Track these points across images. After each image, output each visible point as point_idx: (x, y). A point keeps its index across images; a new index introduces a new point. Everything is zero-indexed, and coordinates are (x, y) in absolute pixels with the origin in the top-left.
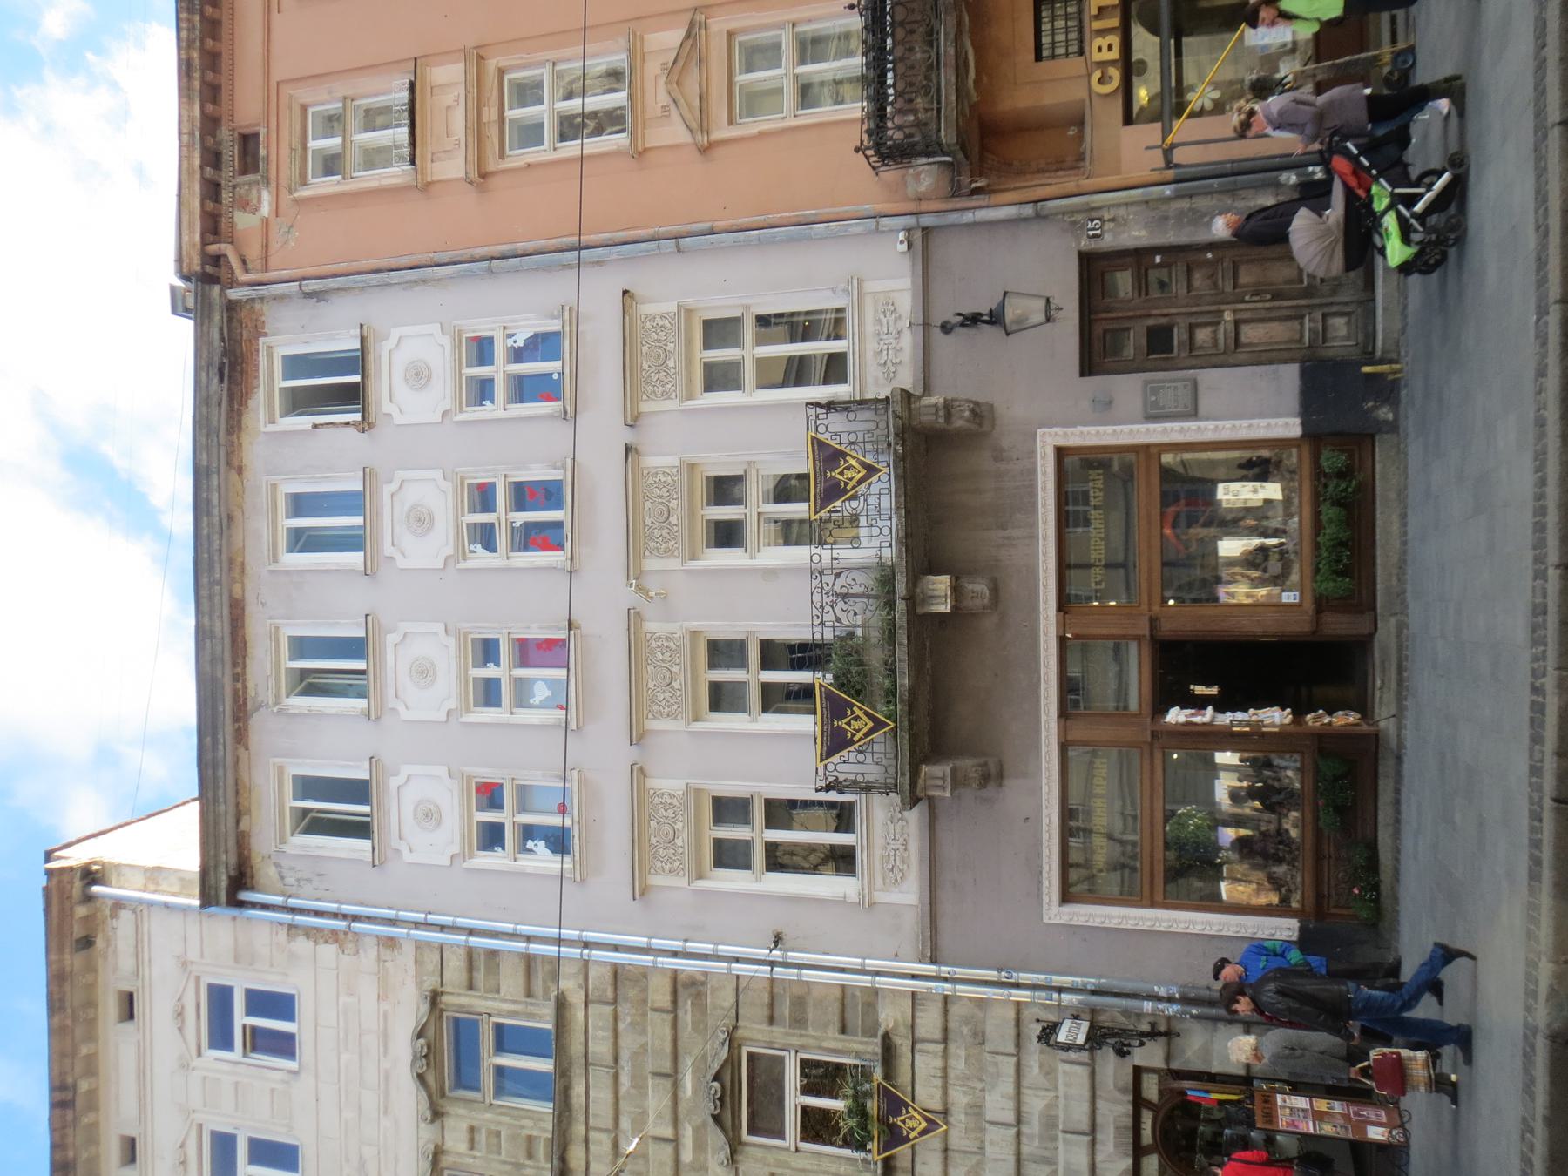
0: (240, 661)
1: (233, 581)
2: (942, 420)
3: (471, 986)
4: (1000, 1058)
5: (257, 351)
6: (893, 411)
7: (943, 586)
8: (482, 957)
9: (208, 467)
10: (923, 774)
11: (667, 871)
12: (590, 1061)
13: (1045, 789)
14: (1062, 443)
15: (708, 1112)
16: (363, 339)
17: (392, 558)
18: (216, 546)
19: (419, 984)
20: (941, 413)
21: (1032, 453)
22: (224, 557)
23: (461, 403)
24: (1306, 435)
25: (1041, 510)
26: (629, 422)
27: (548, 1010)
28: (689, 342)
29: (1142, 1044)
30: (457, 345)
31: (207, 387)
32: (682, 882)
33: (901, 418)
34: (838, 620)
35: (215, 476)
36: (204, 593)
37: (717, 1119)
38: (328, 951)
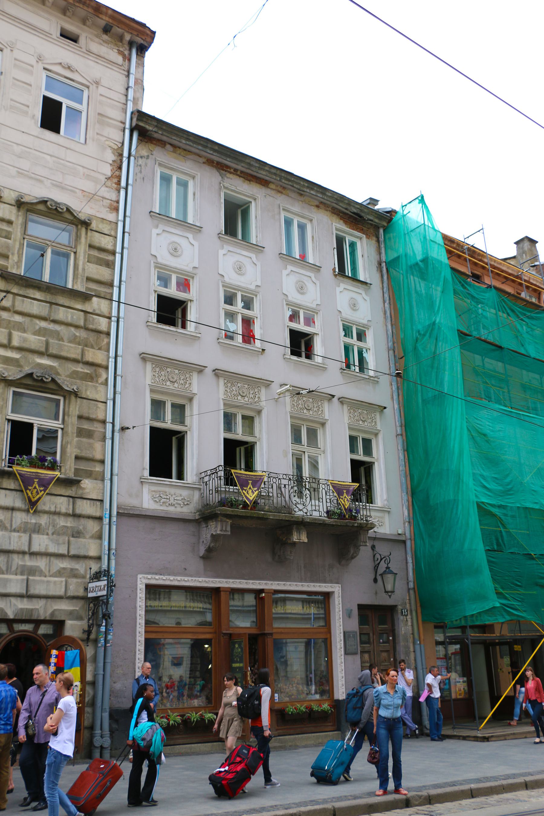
0: (242, 175)
1: (277, 186)
4: (67, 546)
10: (228, 520)
11: (154, 374)
12: (54, 306)
13: (200, 579)
15: (34, 371)
17: (286, 269)
18: (295, 185)
22: (290, 187)
23: (359, 326)
27: (80, 287)
31: (354, 206)
32: (148, 381)
36: (278, 172)
37: (30, 375)
38: (108, 170)
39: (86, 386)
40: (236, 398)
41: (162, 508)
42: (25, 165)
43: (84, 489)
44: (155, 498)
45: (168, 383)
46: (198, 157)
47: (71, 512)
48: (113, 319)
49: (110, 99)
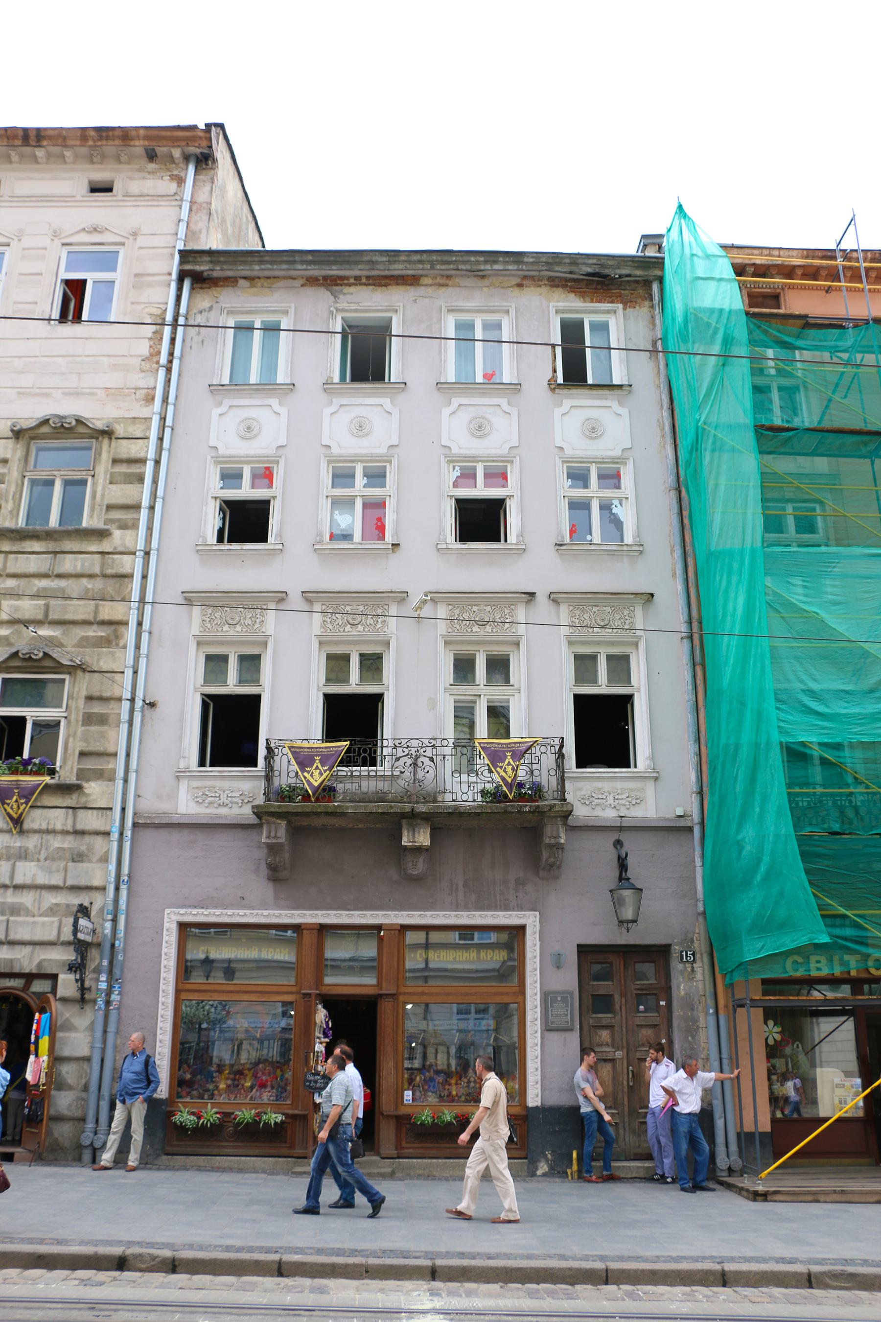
0: (370, 282)
2: (547, 841)
3: (115, 461)
4: (63, 874)
5: (612, 302)
6: (555, 804)
7: (421, 839)
8: (138, 471)
9: (522, 262)
10: (279, 821)
11: (204, 618)
12: (58, 556)
13: (265, 913)
14: (529, 931)
15: (20, 648)
16: (620, 386)
17: (449, 404)
19: (118, 420)
20: (553, 841)
21: (521, 908)
22: (454, 272)
24: (528, 1109)
25: (477, 913)
26: (552, 596)
27: (97, 523)
28: (613, 644)
29: (77, 981)
30: (615, 460)
31: (585, 264)
32: (195, 630)
33: (550, 810)
34: (398, 759)
35: (515, 267)
36: (425, 257)
37: (15, 654)
39: (99, 654)
40: (342, 630)
41: (208, 811)
42: (27, 381)
43: (88, 795)
44: (197, 797)
45: (226, 628)
46: (291, 281)
47: (69, 828)
48: (138, 553)
49: (154, 248)
